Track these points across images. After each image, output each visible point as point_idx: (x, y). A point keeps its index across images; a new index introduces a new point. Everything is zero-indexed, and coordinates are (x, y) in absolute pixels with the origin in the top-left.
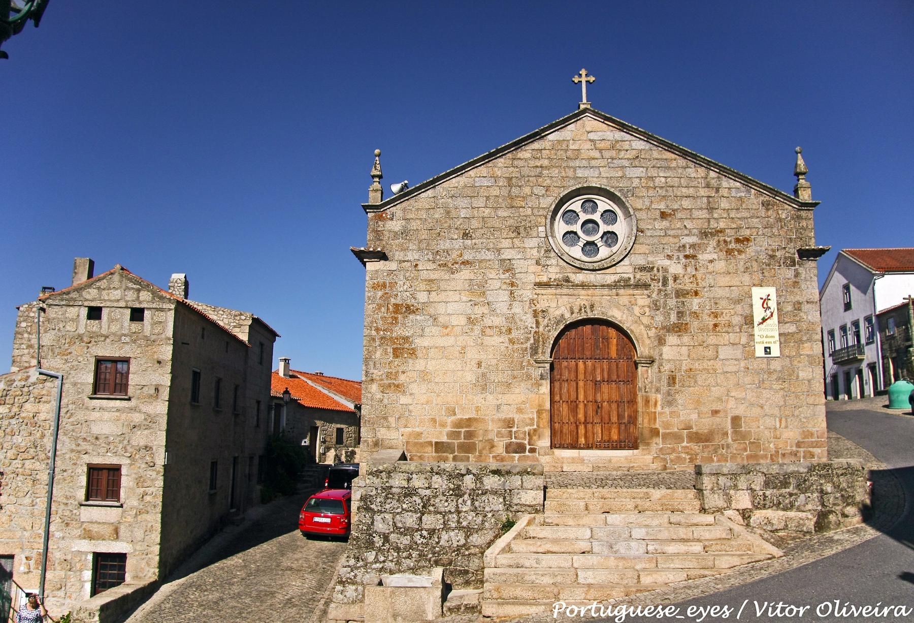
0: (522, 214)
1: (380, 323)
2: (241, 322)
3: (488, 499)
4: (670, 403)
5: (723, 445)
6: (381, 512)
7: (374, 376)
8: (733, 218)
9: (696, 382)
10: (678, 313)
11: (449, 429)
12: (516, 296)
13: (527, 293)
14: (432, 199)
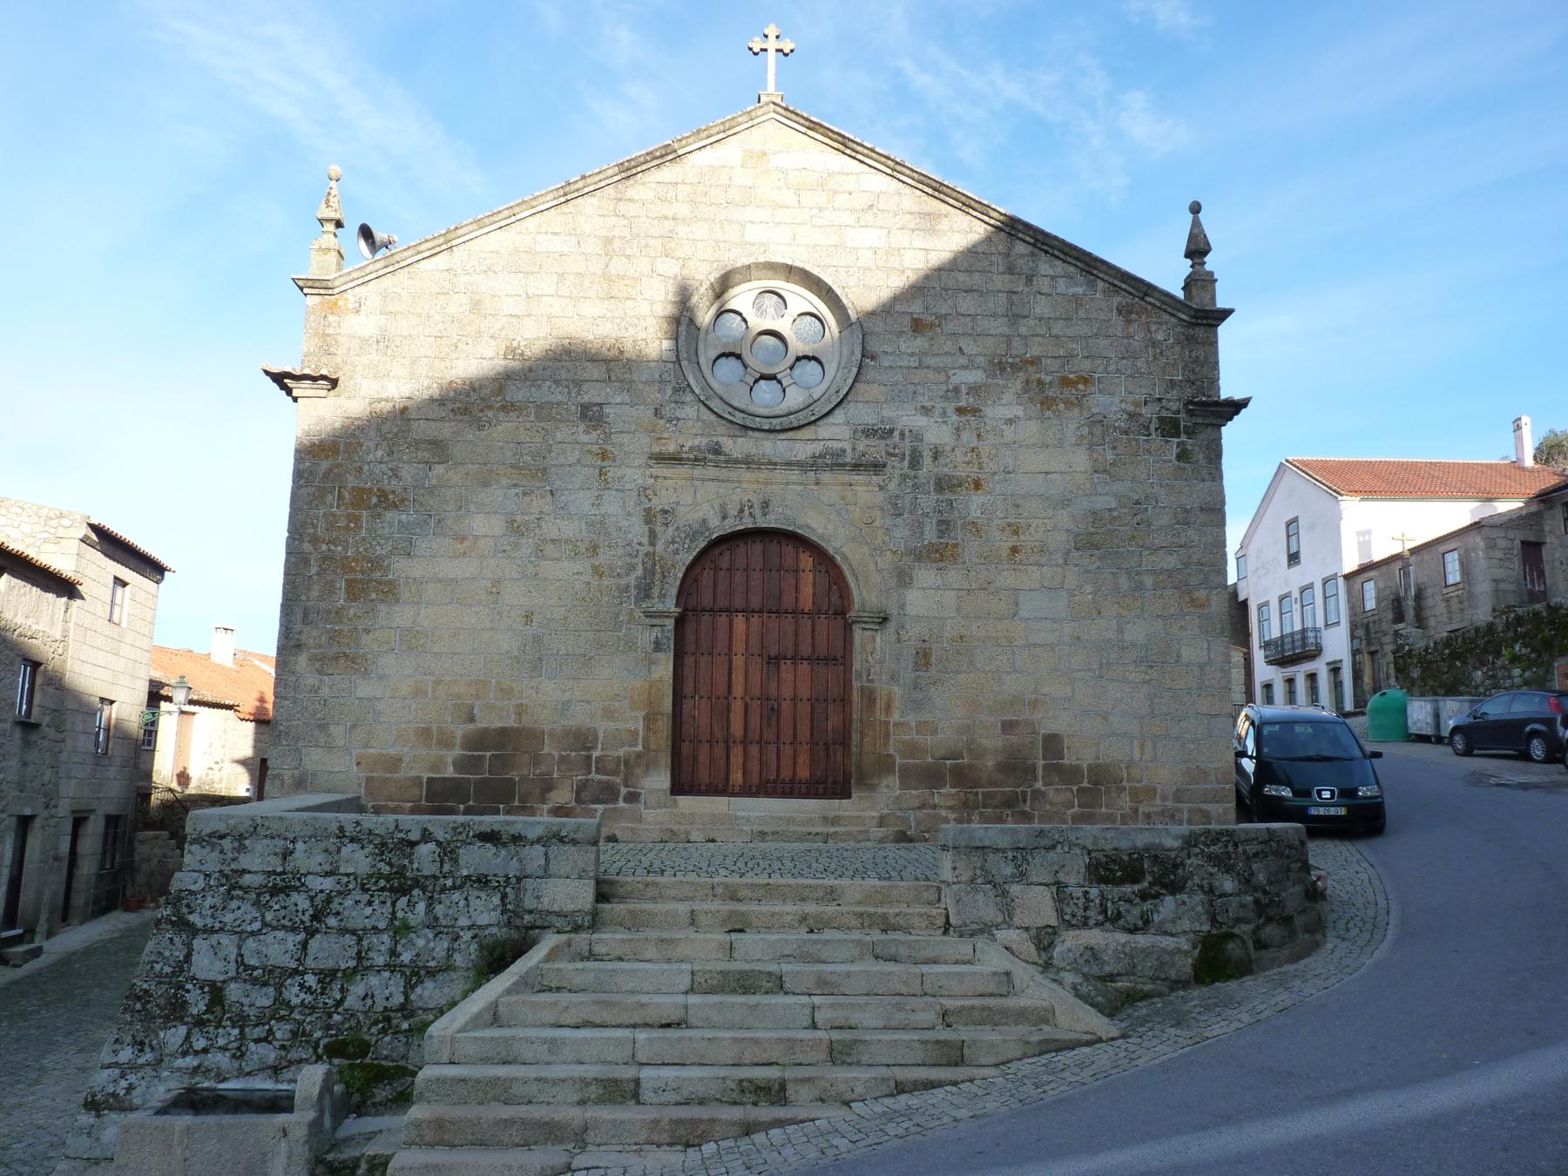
0: (630, 313)
2: (61, 532)
3: (466, 899)
4: (917, 706)
5: (1024, 793)
6: (212, 931)
7: (304, 638)
8: (1057, 337)
9: (971, 663)
10: (940, 522)
11: (458, 752)
12: (609, 480)
13: (634, 474)
14: (445, 275)
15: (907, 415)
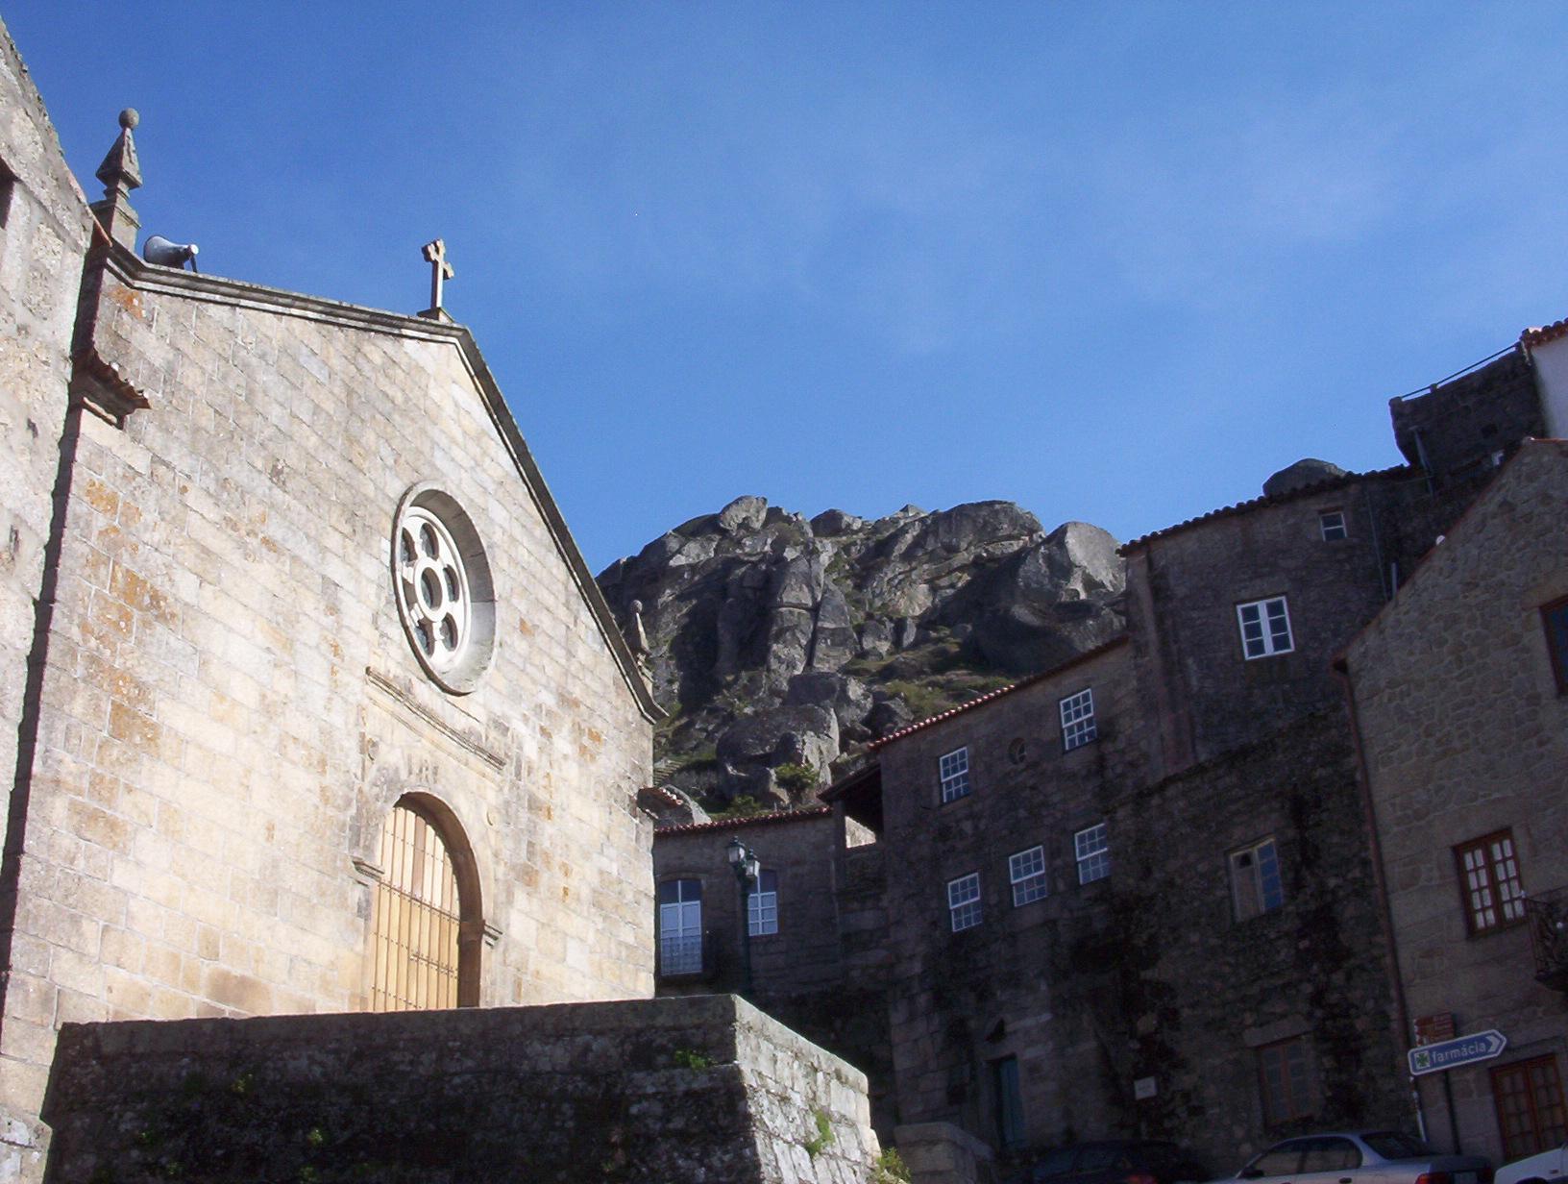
1: (92, 612)
7: (63, 770)
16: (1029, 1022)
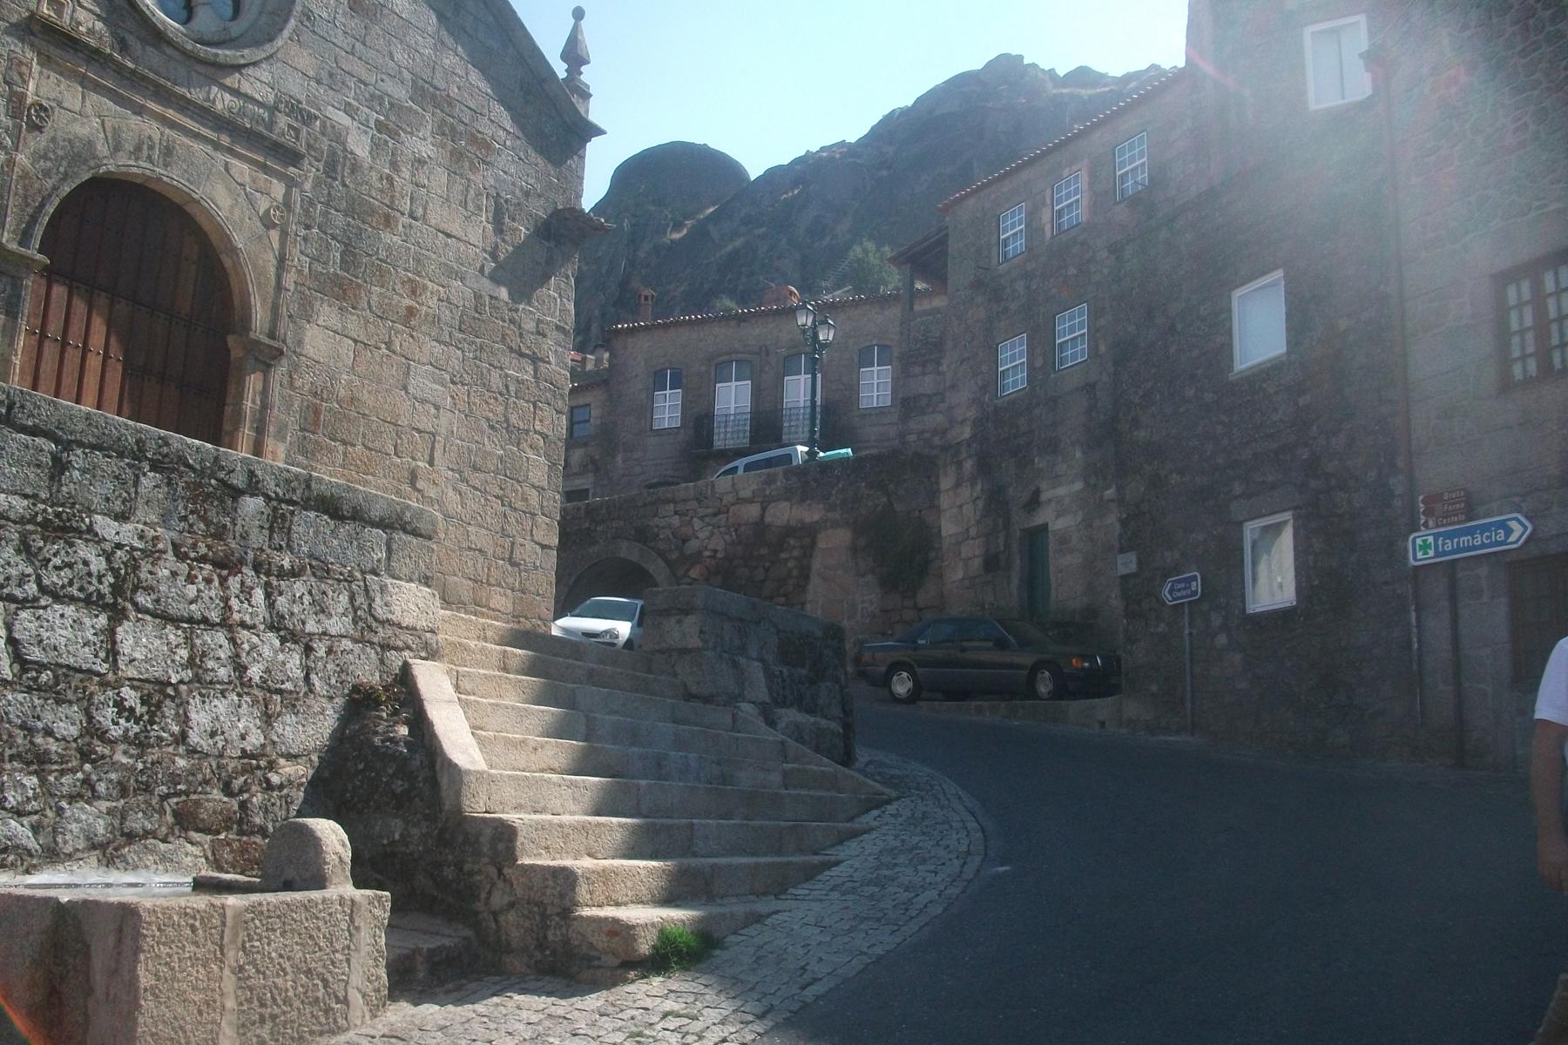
15: (333, 106)
16: (1061, 491)
